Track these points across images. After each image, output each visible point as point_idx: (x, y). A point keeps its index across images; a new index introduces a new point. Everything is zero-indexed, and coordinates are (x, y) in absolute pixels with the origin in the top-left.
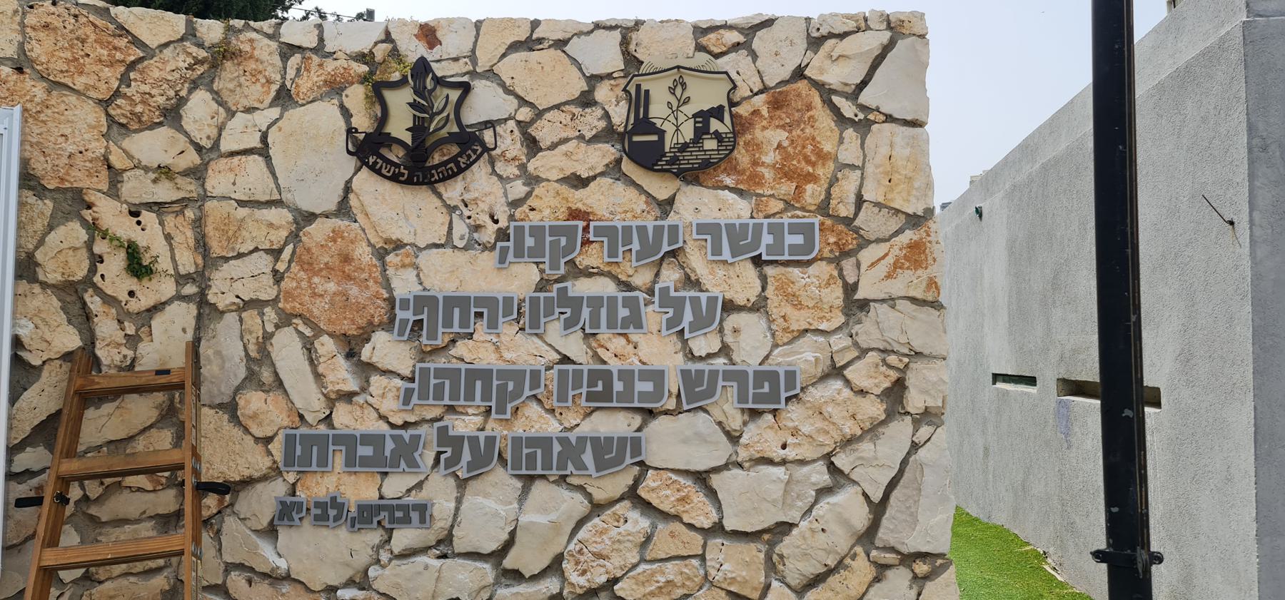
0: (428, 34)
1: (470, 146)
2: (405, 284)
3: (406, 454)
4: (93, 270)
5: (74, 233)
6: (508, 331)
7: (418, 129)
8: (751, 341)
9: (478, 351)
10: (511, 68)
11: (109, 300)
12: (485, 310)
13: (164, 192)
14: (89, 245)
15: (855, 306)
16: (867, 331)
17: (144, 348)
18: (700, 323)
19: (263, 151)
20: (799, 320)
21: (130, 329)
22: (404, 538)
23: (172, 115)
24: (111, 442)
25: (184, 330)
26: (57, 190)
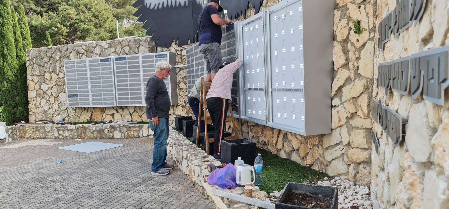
4: (349, 34)
5: (344, 22)
11: (353, 44)
14: (348, 24)
17: (360, 62)
21: (357, 55)
24: (353, 98)
25: (370, 53)
26: (343, 6)
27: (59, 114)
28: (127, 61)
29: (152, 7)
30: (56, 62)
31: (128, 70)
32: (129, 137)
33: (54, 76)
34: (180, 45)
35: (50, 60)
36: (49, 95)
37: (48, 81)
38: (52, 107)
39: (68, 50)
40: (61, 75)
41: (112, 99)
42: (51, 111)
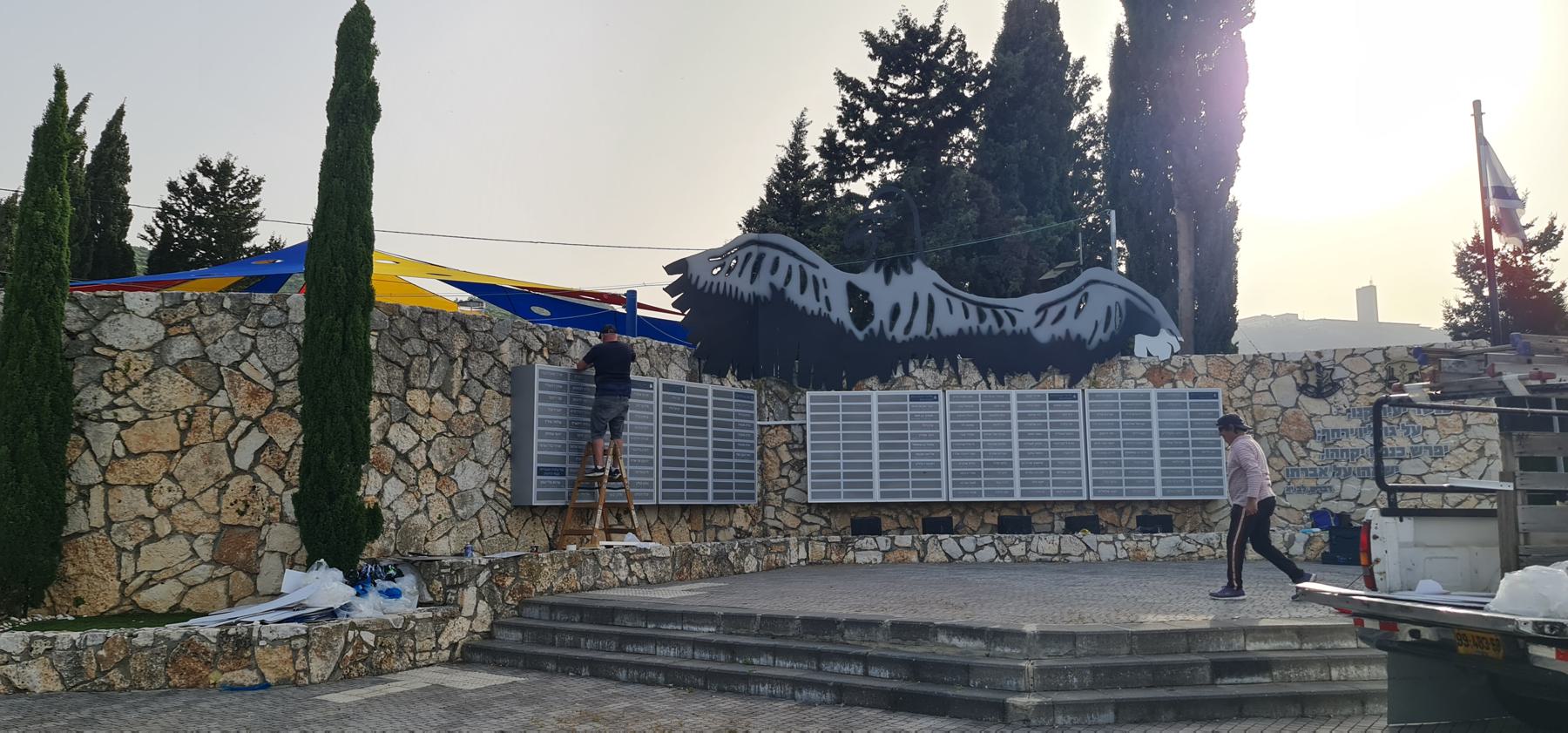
0: (1319, 354)
1: (1335, 386)
2: (1318, 426)
3: (1323, 472)
6: (1352, 438)
7: (1319, 382)
8: (1433, 438)
9: (1344, 444)
10: (1346, 363)
12: (1346, 432)
13: (1243, 404)
15: (1466, 427)
16: (1471, 434)
18: (1416, 433)
19: (1270, 390)
20: (1448, 431)
22: (1325, 496)
23: (1242, 382)
27: (447, 534)
28: (685, 395)
29: (700, 285)
30: (453, 360)
31: (685, 416)
32: (769, 569)
33: (440, 403)
34: (739, 379)
35: (428, 355)
36: (419, 466)
37: (421, 420)
38: (426, 508)
39: (496, 332)
40: (466, 405)
41: (650, 485)
42: (420, 519)
